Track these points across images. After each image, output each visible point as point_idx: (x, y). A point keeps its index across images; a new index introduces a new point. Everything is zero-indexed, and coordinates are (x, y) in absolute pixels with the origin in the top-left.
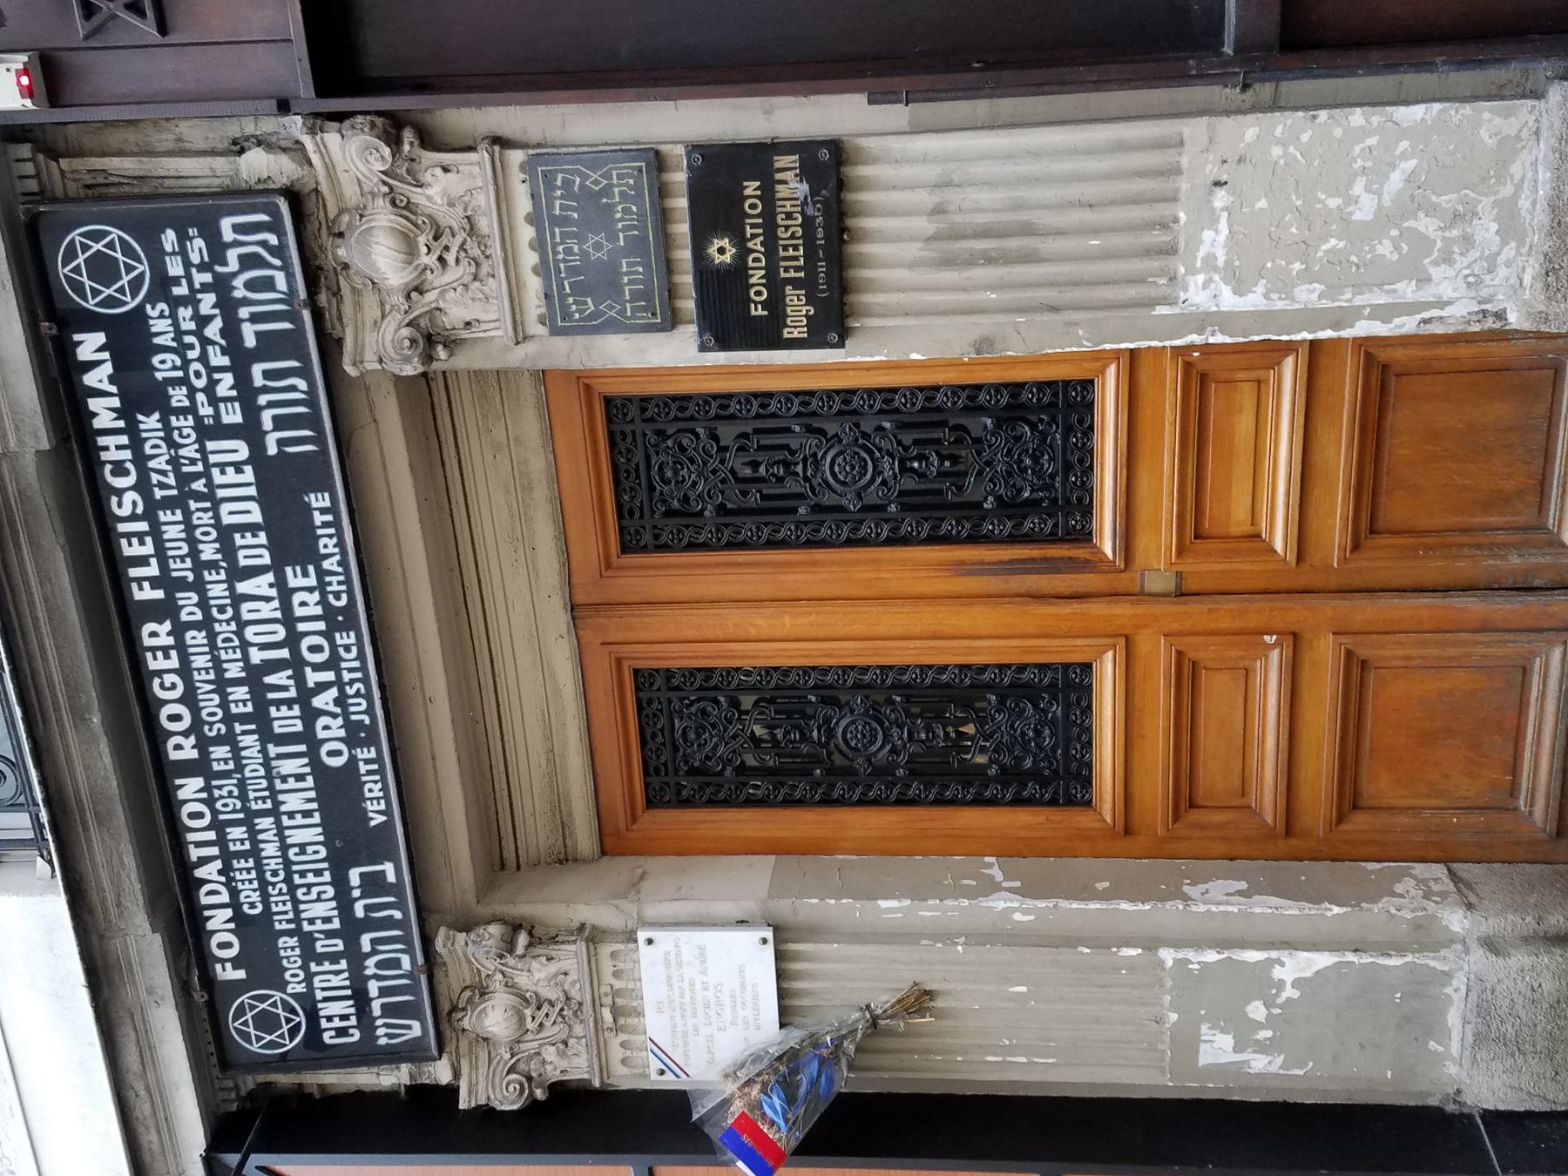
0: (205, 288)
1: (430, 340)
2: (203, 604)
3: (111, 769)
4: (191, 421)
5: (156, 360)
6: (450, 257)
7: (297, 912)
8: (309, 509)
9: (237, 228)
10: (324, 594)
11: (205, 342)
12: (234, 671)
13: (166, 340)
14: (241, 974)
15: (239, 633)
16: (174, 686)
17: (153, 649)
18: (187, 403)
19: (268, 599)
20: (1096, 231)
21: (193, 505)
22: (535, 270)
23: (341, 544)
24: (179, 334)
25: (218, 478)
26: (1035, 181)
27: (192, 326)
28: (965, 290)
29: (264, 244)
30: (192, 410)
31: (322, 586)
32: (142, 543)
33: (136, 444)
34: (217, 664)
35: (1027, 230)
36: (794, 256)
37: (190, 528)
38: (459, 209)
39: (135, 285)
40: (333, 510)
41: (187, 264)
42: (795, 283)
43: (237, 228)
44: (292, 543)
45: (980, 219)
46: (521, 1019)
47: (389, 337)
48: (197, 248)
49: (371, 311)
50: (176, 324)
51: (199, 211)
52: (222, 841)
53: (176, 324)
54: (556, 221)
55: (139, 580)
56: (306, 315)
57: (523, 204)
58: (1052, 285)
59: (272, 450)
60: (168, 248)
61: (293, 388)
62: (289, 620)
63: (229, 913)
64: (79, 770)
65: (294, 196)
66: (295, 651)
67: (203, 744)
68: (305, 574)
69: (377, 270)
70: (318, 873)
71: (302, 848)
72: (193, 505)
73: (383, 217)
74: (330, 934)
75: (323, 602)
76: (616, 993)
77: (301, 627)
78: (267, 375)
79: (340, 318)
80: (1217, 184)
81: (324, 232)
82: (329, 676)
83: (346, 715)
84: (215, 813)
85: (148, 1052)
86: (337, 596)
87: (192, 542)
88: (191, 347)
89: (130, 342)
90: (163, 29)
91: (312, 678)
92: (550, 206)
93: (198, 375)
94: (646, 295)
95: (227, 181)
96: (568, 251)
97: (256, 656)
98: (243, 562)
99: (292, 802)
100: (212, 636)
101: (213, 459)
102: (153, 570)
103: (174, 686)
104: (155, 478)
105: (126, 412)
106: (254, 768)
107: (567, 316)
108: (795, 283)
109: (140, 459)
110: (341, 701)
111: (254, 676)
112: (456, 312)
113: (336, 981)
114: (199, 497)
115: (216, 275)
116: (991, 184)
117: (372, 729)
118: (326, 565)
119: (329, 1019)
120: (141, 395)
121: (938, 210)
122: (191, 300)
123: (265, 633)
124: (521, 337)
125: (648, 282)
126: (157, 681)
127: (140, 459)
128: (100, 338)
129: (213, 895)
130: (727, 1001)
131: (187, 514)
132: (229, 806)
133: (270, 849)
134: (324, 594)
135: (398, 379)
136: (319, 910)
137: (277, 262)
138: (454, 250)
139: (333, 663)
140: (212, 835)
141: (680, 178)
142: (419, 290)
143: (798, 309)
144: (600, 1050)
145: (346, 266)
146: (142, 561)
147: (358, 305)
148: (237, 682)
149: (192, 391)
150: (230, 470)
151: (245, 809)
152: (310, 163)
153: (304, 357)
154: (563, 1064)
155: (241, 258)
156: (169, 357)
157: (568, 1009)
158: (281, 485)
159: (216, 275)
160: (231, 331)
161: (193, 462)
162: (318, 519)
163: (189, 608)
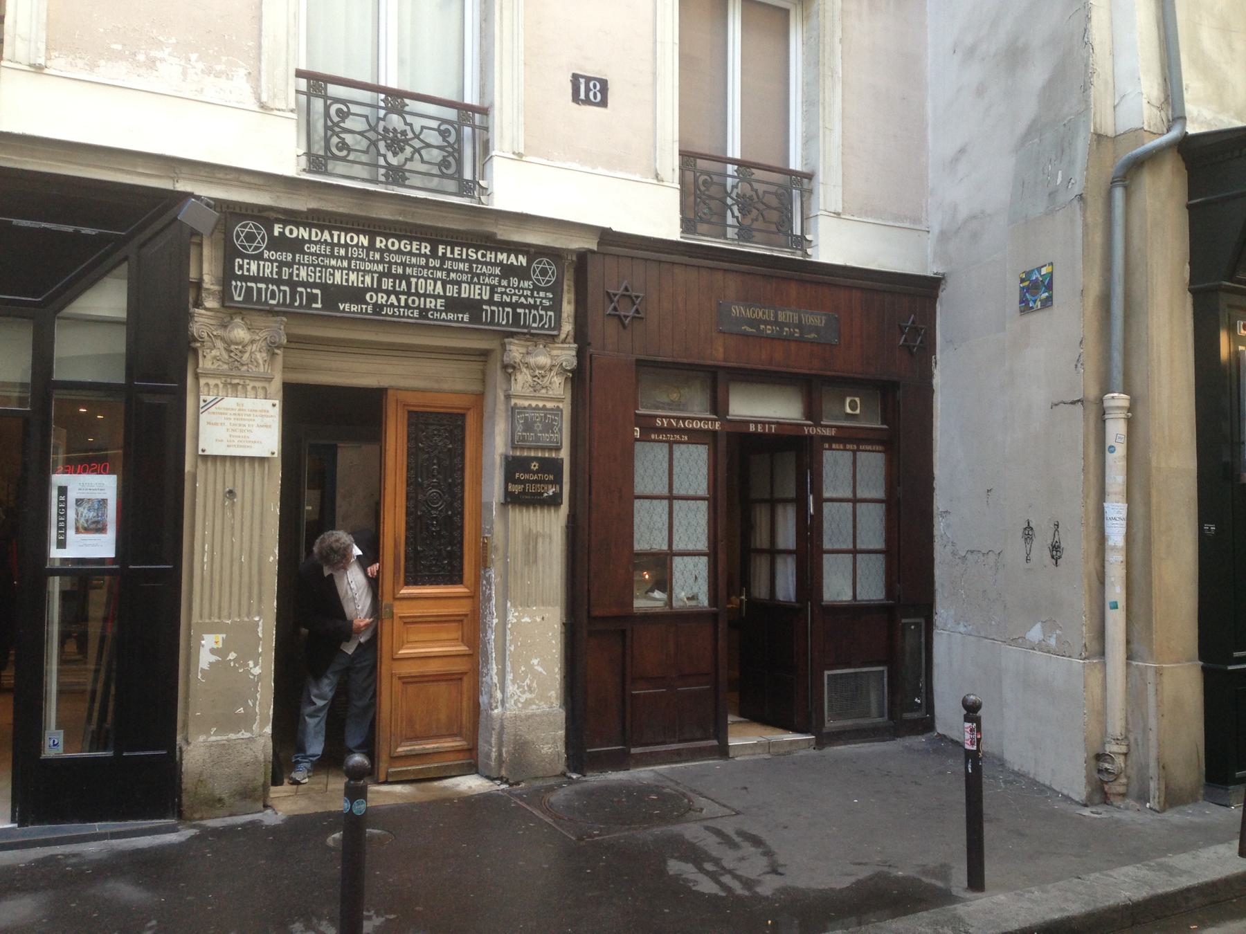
2: (434, 268)
7: (303, 265)
12: (408, 271)
14: (276, 233)
15: (422, 277)
36: (532, 489)
44: (454, 304)
46: (237, 344)
48: (548, 304)
52: (339, 245)
62: (426, 296)
63: (306, 237)
66: (413, 294)
67: (381, 251)
70: (320, 278)
71: (333, 275)
74: (291, 275)
75: (430, 309)
76: (244, 386)
82: (403, 304)
83: (387, 306)
84: (352, 246)
85: (250, 187)
87: (457, 271)
89: (522, 273)
91: (403, 298)
97: (413, 280)
99: (353, 277)
100: (423, 267)
105: (501, 264)
106: (369, 266)
109: (486, 264)
110: (392, 305)
111: (407, 278)
112: (520, 377)
113: (268, 271)
114: (472, 278)
117: (379, 314)
119: (249, 264)
120: (508, 271)
122: (532, 296)
127: (486, 264)
129: (315, 234)
130: (247, 434)
132: (354, 253)
133: (333, 262)
136: (303, 273)
139: (407, 306)
140: (342, 242)
143: (516, 489)
144: (214, 375)
146: (452, 252)
148: (404, 270)
151: (352, 258)
153: (512, 326)
154: (208, 357)
157: (236, 364)
158: (473, 307)
160: (522, 306)
163: (432, 262)
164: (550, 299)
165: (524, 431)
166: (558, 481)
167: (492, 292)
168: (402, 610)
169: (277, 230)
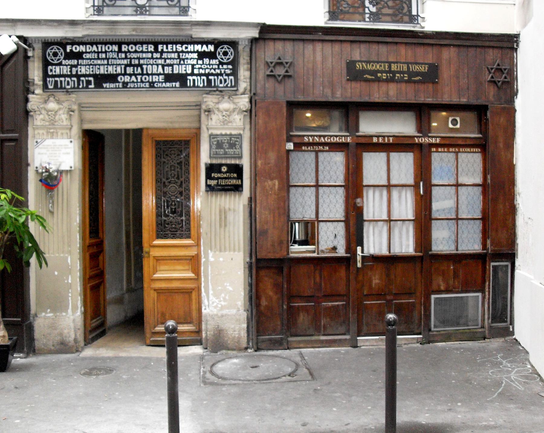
0: (221, 71)
2: (157, 58)
6: (224, 117)
8: (176, 82)
11: (211, 69)
15: (150, 64)
17: (148, 46)
34: (144, 59)
35: (225, 226)
36: (223, 182)
37: (173, 59)
39: (222, 59)
40: (175, 87)
41: (225, 69)
48: (228, 72)
56: (215, 89)
62: (152, 74)
64: (123, 27)
75: (156, 82)
89: (212, 55)
97: (145, 67)
100: (150, 59)
107: (213, 138)
108: (218, 182)
109: (188, 52)
112: (214, 117)
120: (202, 55)
121: (230, 209)
122: (219, 68)
125: (219, 154)
127: (188, 52)
128: (213, 50)
131: (176, 59)
141: (237, 162)
146: (167, 48)
162: (174, 84)
163: (155, 55)
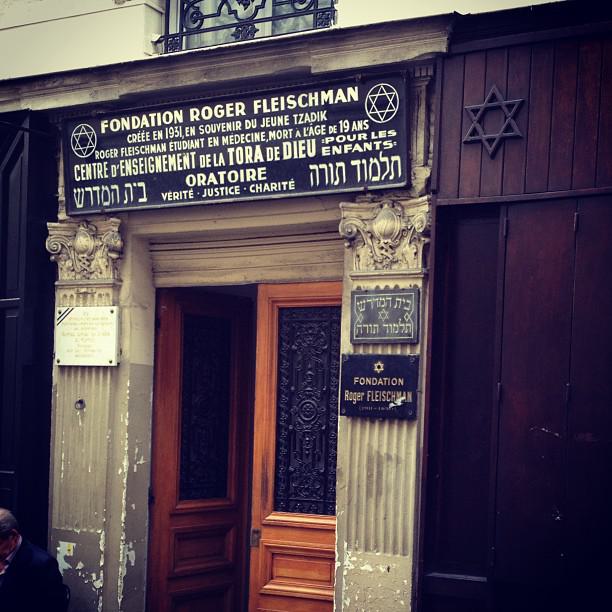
0: (374, 146)
1: (353, 239)
2: (252, 130)
3: (184, 84)
4: (323, 133)
5: (346, 121)
6: (383, 252)
7: (128, 158)
8: (289, 180)
9: (396, 162)
10: (255, 183)
11: (353, 143)
13: (354, 127)
14: (103, 131)
15: (240, 145)
16: (219, 114)
17: (234, 107)
18: (330, 133)
19: (253, 158)
20: (376, 520)
21: (291, 130)
22: (378, 287)
23: (274, 192)
24: (357, 133)
25: (301, 142)
26: (396, 498)
27: (360, 139)
28: (359, 466)
29: (390, 173)
30: (328, 135)
31: (258, 182)
32: (276, 107)
33: (315, 109)
34: (228, 134)
35: (379, 493)
36: (375, 397)
37: (282, 128)
38: (400, 258)
39: (375, 116)
40: (288, 191)
41: (383, 140)
42: (365, 396)
43: (396, 162)
44: (277, 171)
45: (384, 473)
46: (83, 253)
47: (354, 222)
48: (389, 145)
49: (365, 215)
50: (361, 132)
51: (404, 147)
52: (157, 128)
53: (361, 132)
54: (394, 298)
55: (261, 104)
56: (362, 189)
57: (403, 284)
58: (358, 501)
59: (312, 167)
60: (389, 132)
61: (335, 179)
62: (245, 166)
63: (128, 128)
64: (187, 70)
65: (409, 187)
66: (233, 168)
67: (196, 124)
68: (263, 176)
69: (380, 220)
70: (143, 168)
71: (153, 163)
72: (291, 130)
73: (398, 225)
74: (118, 171)
75: (252, 182)
76: (93, 294)
77: (242, 171)
78: (340, 168)
79: (362, 202)
80: (388, 569)
81: (395, 198)
82: (222, 182)
83: (207, 187)
84: (168, 126)
85: (73, 88)
86: (254, 188)
88: (352, 138)
89: (353, 111)
90: (466, 142)
91: (222, 174)
92: (400, 297)
93: (341, 139)
94: (364, 334)
95: (414, 158)
96: (382, 303)
97: (231, 151)
98: (268, 149)
99: (172, 160)
100: (239, 132)
101: (308, 141)
102: (266, 110)
103: (219, 114)
104: (302, 115)
106: (186, 145)
107: (359, 299)
108: (365, 396)
109: (309, 110)
112: (363, 251)
113: (100, 172)
114: (294, 133)
115: (379, 151)
116: (397, 478)
117: (199, 197)
118: (266, 185)
119: (84, 168)
120: (336, 113)
121: (389, 457)
122: (369, 140)
123: (242, 155)
124: (356, 278)
125: (369, 335)
126: (222, 107)
127: (309, 110)
128: (356, 98)
130: (88, 343)
131: (287, 128)
132: (172, 132)
134: (255, 183)
135: (339, 221)
136: (128, 168)
137: (383, 178)
138: (385, 253)
139: (227, 184)
140: (159, 124)
141: (408, 352)
142: (372, 237)
144: (70, 286)
145: (381, 206)
146: (269, 107)
147: (367, 209)
149: (335, 135)
150: (304, 148)
152: (421, 196)
153: (346, 185)
154: (65, 269)
155: (385, 163)
156: (348, 127)
157: (87, 273)
158: (295, 170)
159: (379, 151)
161: (307, 132)
162: (285, 183)
163: (251, 124)
164: (393, 139)
165: (365, 322)
166: (411, 386)
167: (319, 146)
168: (269, 538)
169: (104, 126)
